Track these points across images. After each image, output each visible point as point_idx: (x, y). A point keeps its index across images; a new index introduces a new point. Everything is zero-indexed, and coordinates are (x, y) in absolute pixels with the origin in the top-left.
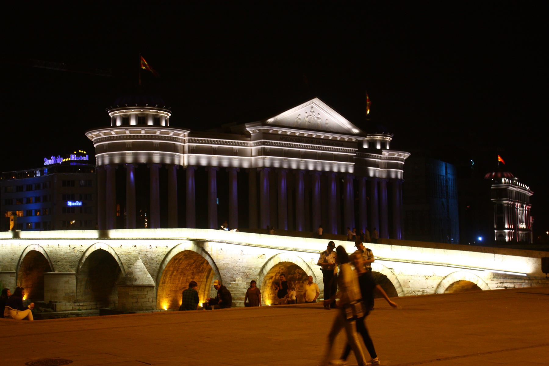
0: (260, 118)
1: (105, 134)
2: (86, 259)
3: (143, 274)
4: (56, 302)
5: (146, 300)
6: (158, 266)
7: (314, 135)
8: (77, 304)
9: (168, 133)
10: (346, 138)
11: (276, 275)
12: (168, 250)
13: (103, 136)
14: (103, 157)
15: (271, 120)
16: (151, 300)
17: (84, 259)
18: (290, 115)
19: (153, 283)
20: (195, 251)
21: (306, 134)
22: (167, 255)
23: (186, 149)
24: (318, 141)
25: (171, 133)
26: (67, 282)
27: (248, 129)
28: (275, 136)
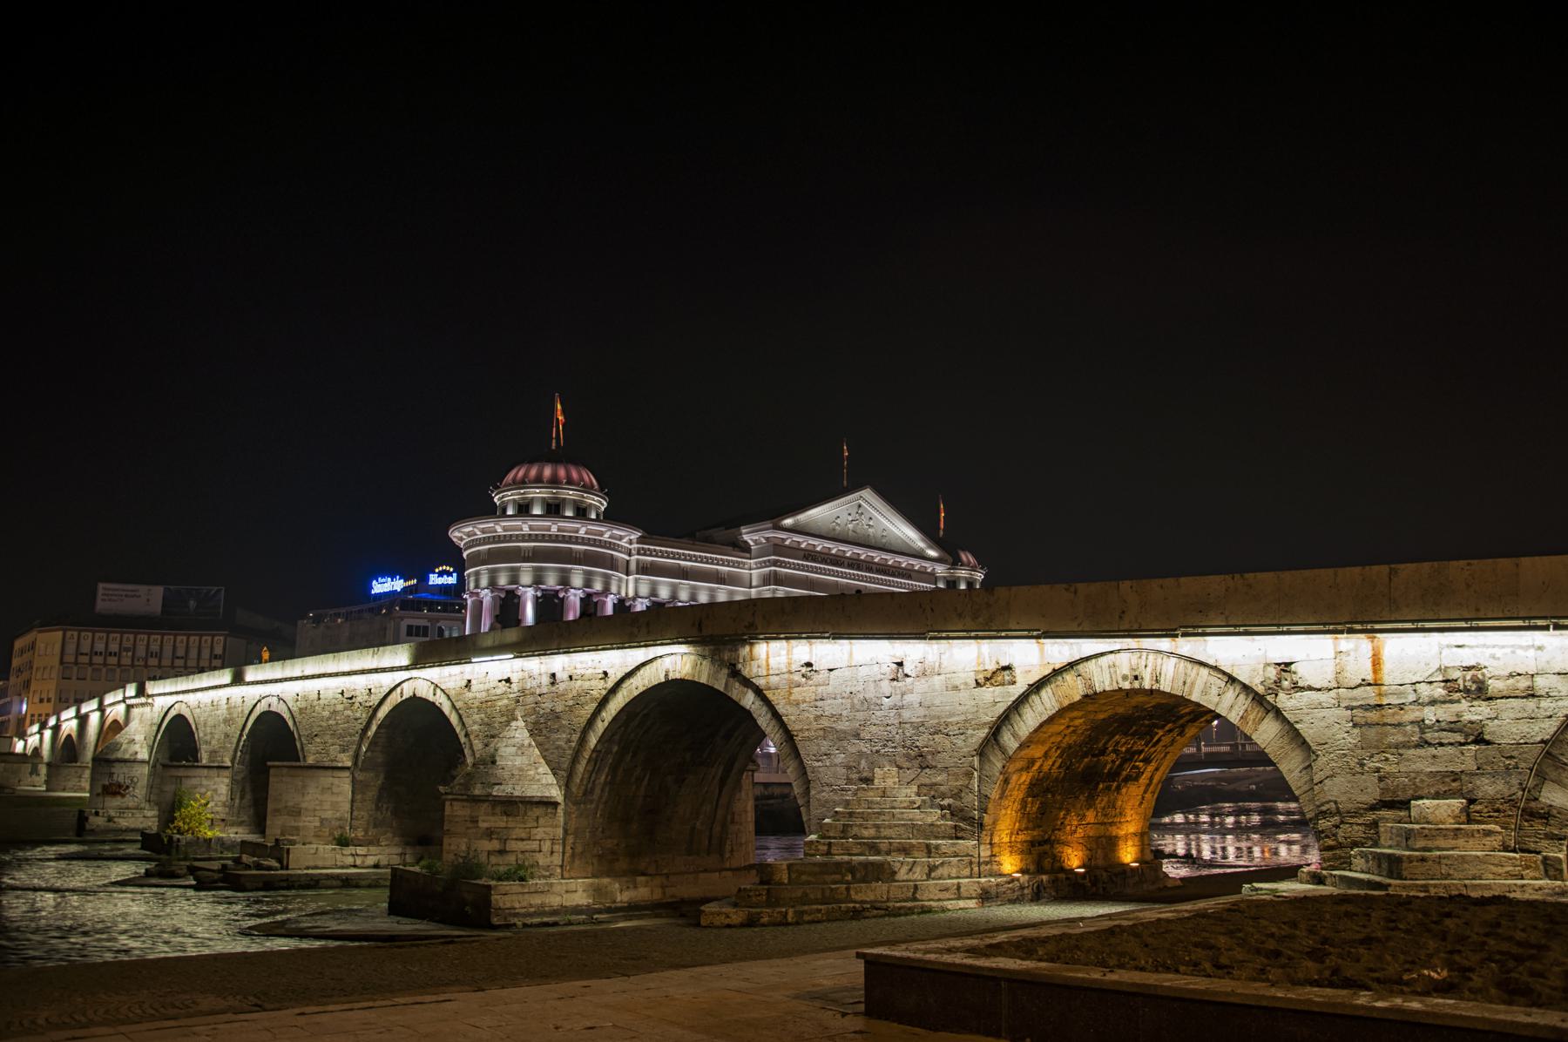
0: (771, 515)
1: (483, 531)
2: (379, 727)
3: (527, 769)
4: (293, 843)
5: (535, 845)
6: (575, 737)
7: (863, 554)
8: (348, 850)
9: (601, 534)
10: (917, 564)
11: (1046, 755)
12: (610, 683)
13: (480, 535)
14: (477, 574)
15: (788, 522)
16: (546, 846)
17: (374, 728)
18: (818, 514)
19: (556, 793)
20: (703, 680)
21: (849, 551)
22: (603, 702)
23: (633, 566)
24: (869, 566)
25: (608, 533)
26: (328, 789)
27: (746, 537)
28: (794, 551)
